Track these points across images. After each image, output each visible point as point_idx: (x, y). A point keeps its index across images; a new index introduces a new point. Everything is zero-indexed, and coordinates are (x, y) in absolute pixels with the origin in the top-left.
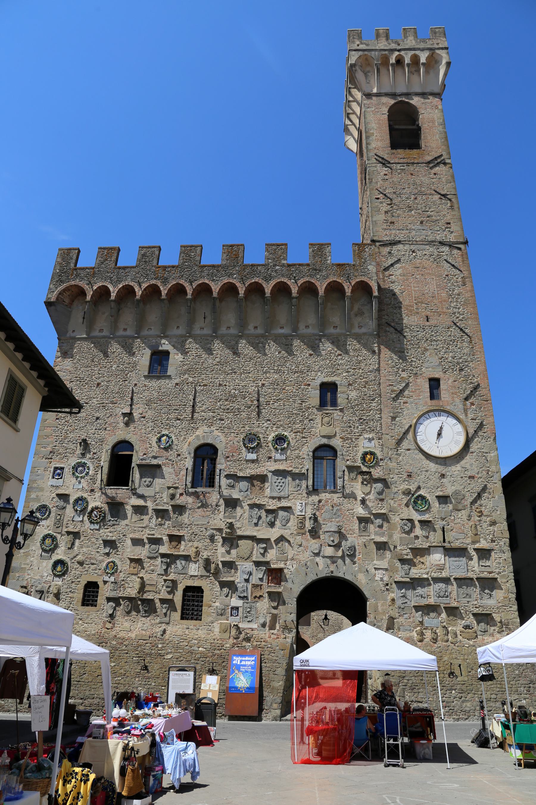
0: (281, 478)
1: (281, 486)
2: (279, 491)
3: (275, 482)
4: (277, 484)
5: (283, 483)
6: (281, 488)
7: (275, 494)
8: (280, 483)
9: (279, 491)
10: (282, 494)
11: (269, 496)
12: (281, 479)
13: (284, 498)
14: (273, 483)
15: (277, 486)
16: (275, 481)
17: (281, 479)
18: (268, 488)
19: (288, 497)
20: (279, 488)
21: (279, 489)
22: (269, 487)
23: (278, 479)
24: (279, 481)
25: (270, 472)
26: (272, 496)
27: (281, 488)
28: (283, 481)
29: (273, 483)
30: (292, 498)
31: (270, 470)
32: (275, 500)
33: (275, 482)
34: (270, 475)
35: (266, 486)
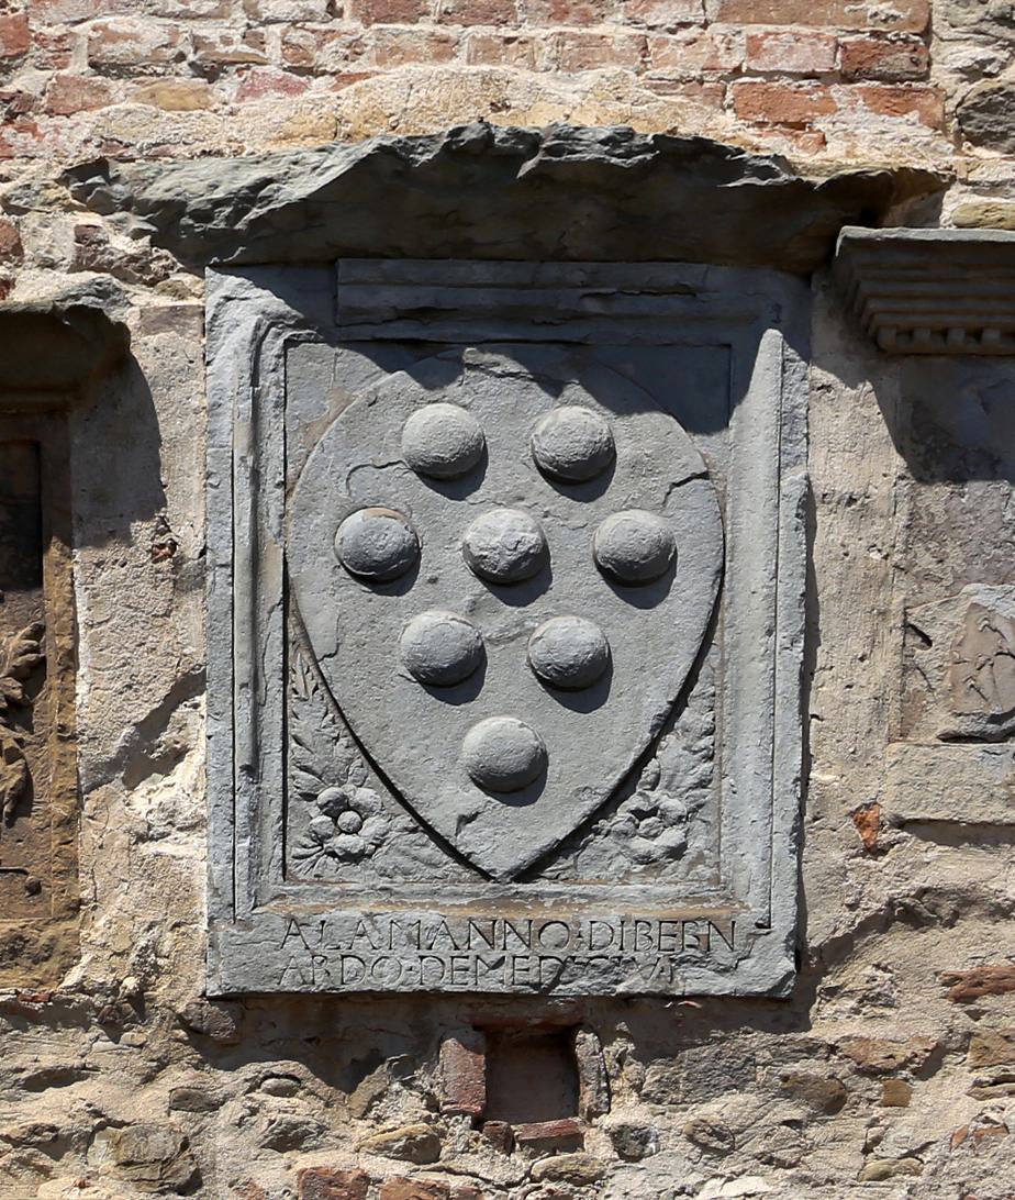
0: (572, 420)
1: (580, 684)
2: (503, 839)
3: (389, 574)
4: (430, 622)
5: (639, 578)
6: (589, 752)
7: (393, 933)
8: (520, 579)
9: (503, 839)
10: (615, 913)
11: (191, 985)
12: (583, 477)
13: (667, 1026)
14: (330, 605)
15: (454, 680)
16: (376, 530)
17: (583, 477)
18: (146, 755)
19: (782, 1009)
20: (498, 726)
21: (515, 784)
22: (199, 728)
23: (456, 474)
24: (497, 524)
25: (193, 236)
26: (294, 967)
27: (589, 752)
28: (622, 524)
29: (330, 605)
30: (920, 1020)
31: (191, 181)
32: (405, 1113)
33: (389, 574)
34: (206, 347)
35: (98, 701)
